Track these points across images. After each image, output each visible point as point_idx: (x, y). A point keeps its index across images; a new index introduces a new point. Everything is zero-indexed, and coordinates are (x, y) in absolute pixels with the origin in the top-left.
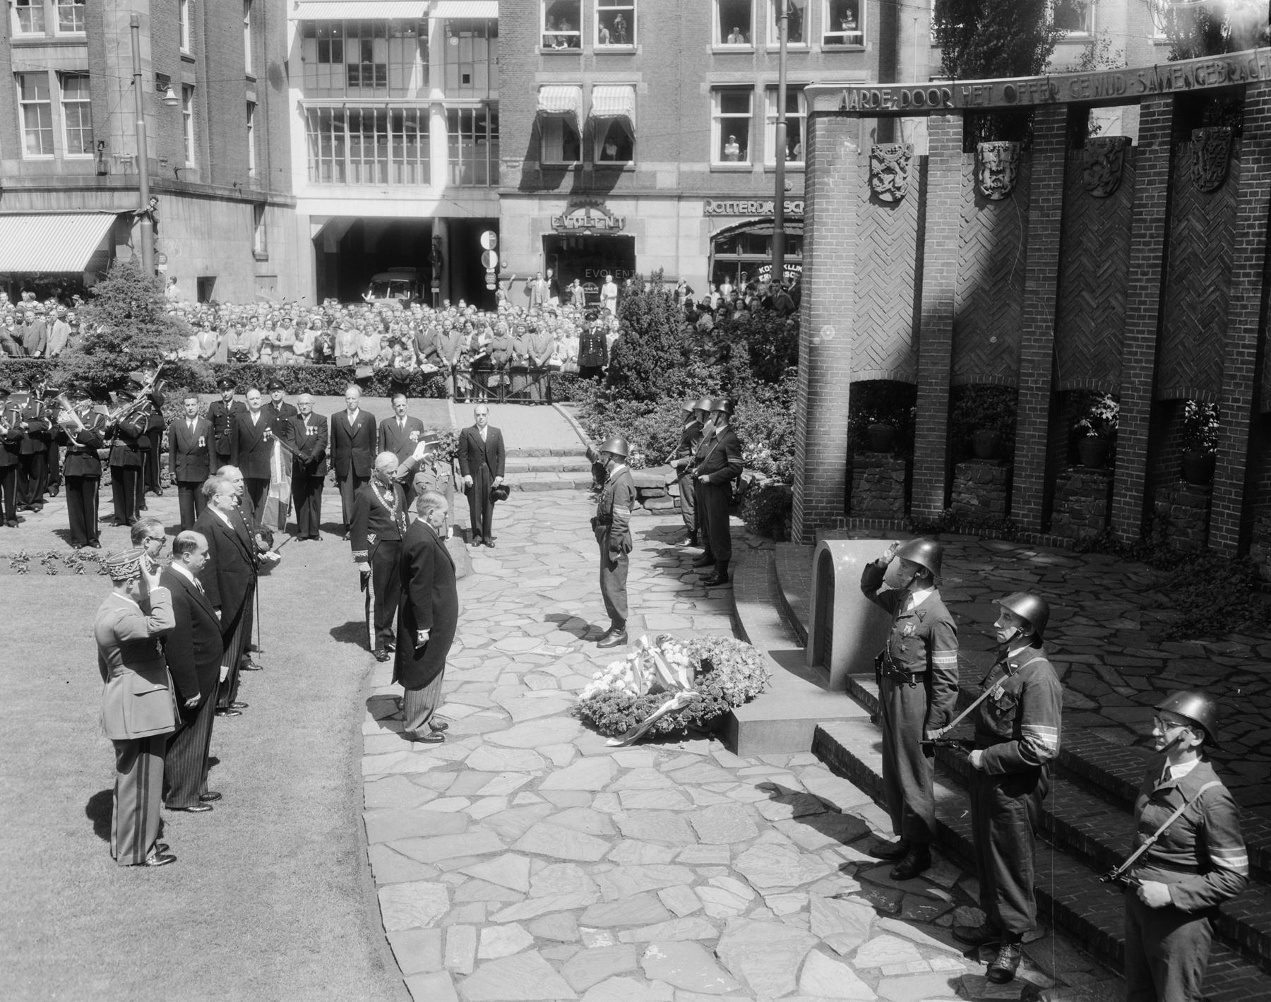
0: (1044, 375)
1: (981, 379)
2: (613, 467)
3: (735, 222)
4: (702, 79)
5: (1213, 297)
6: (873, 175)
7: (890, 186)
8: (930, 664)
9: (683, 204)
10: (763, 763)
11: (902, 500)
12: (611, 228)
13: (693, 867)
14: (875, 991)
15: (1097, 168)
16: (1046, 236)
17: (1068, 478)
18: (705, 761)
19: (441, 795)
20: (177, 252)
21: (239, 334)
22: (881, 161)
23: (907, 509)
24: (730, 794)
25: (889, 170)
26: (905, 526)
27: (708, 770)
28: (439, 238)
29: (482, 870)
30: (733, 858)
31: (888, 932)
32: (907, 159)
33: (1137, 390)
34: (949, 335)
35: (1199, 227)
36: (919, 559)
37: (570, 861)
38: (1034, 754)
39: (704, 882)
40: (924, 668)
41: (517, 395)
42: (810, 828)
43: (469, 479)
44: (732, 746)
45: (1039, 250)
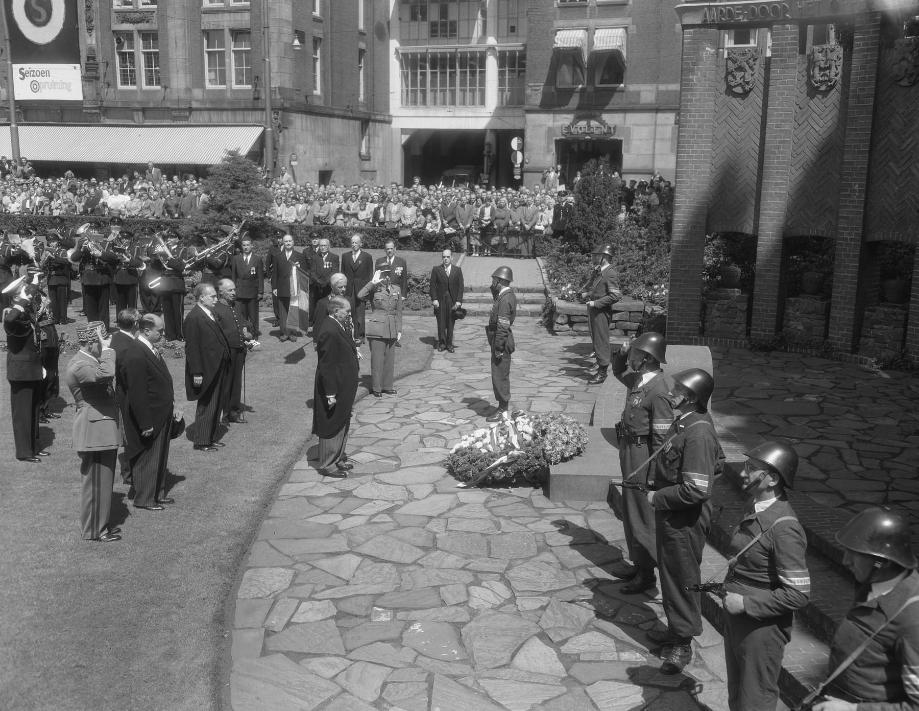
0: (856, 229)
2: (500, 289)
6: (729, 73)
7: (741, 81)
8: (651, 429)
9: (659, 115)
10: (566, 506)
11: (744, 325)
12: (605, 134)
13: (476, 573)
14: (567, 670)
17: (874, 311)
18: (523, 502)
19: (326, 512)
20: (305, 153)
21: (321, 205)
22: (734, 62)
23: (748, 333)
24: (531, 526)
25: (741, 69)
26: (746, 345)
27: (523, 509)
28: (489, 144)
29: (325, 564)
30: (509, 568)
31: (598, 629)
32: (755, 60)
36: (647, 350)
37: (390, 562)
38: (689, 495)
39: (478, 583)
40: (647, 433)
41: (512, 251)
42: (577, 553)
43: (436, 302)
44: (547, 494)
45: (855, 130)
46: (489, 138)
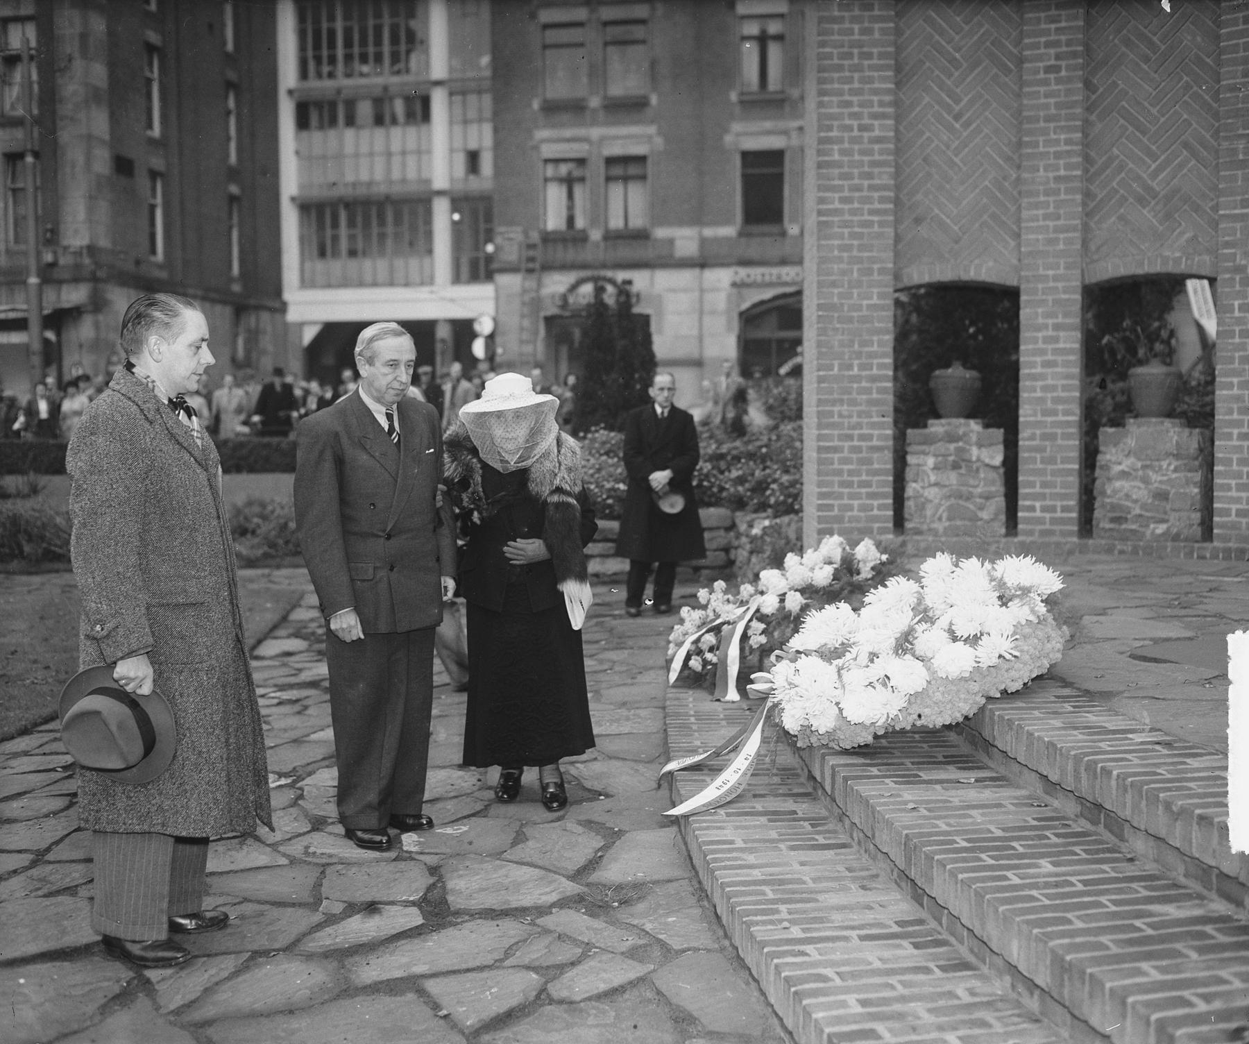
3: (768, 294)
4: (726, 131)
11: (1000, 501)
28: (443, 341)
46: (443, 333)
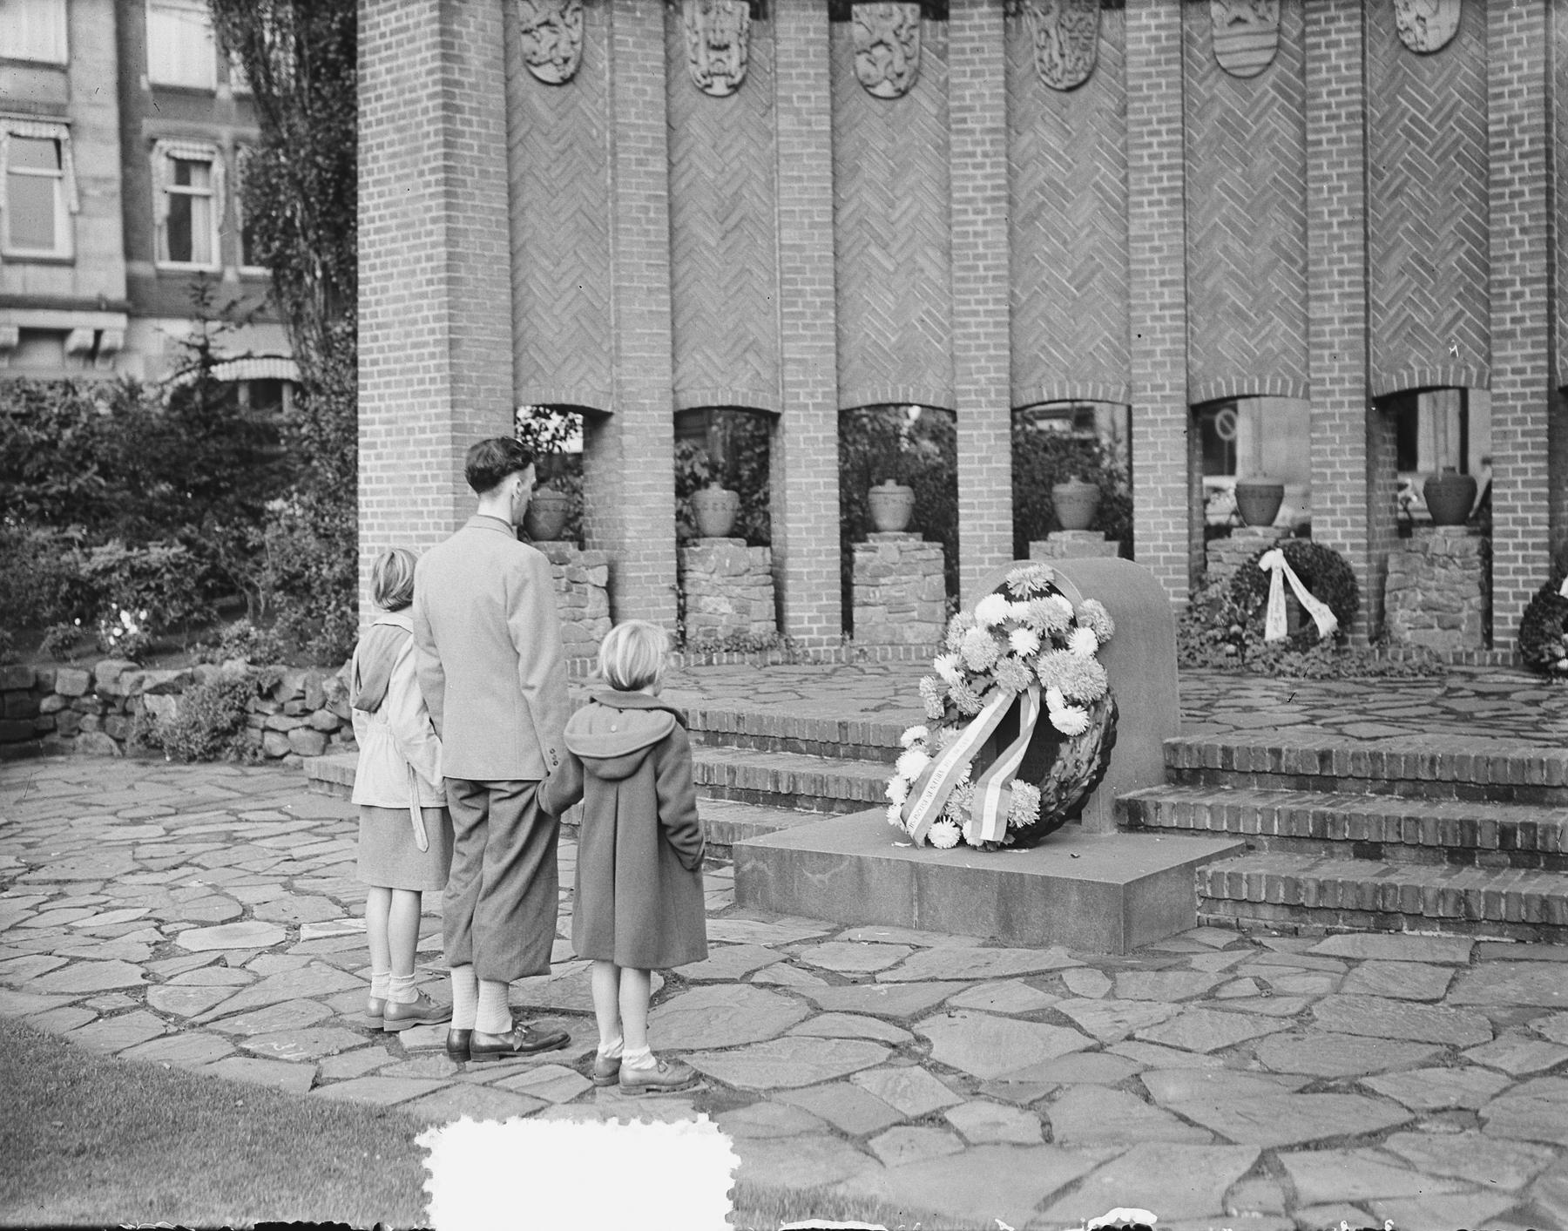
0: (823, 383)
1: (714, 396)
5: (1090, 242)
15: (880, 51)
16: (810, 156)
33: (985, 393)
34: (668, 321)
35: (1053, 142)
45: (800, 179)
